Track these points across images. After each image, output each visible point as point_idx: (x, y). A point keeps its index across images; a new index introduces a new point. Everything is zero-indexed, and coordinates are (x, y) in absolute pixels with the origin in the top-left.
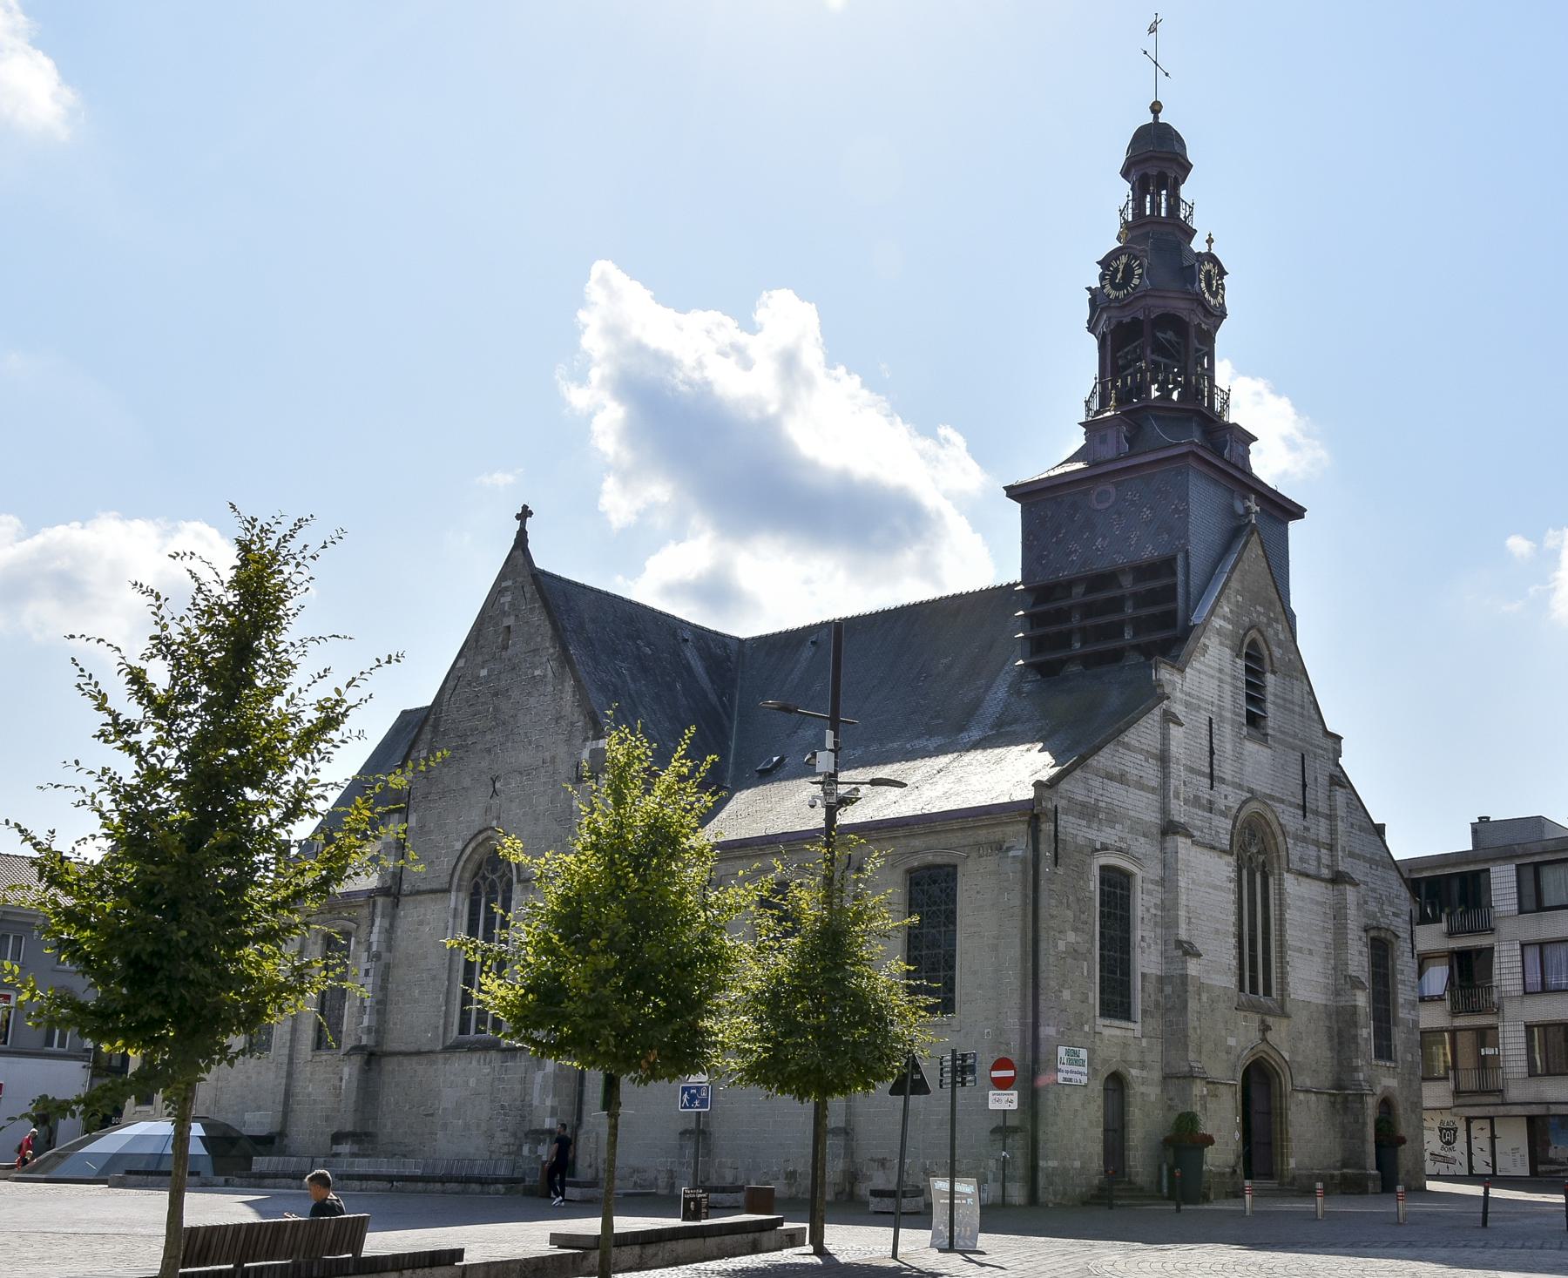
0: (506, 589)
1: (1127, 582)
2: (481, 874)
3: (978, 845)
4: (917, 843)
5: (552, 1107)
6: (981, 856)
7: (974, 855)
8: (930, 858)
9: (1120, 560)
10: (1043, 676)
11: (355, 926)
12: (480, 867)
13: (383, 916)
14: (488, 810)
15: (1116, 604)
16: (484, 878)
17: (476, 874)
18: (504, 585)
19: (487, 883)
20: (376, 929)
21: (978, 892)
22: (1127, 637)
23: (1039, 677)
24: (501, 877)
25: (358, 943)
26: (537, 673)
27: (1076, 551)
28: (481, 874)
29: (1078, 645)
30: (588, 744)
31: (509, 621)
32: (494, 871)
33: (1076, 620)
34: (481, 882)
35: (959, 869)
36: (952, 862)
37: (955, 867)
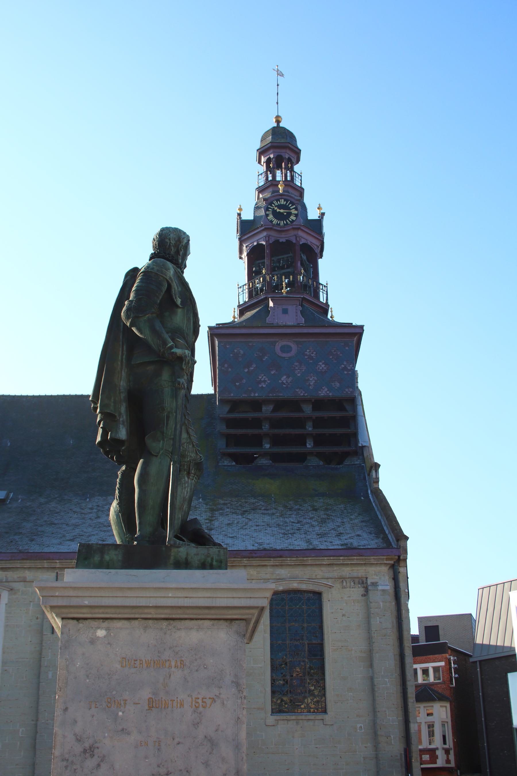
1: (308, 409)
3: (342, 579)
4: (283, 572)
6: (344, 587)
7: (338, 585)
8: (295, 585)
9: (301, 393)
10: (237, 463)
21: (343, 615)
22: (308, 446)
23: (234, 463)
27: (265, 381)
29: (267, 446)
33: (266, 428)
35: (325, 597)
36: (316, 589)
37: (318, 595)
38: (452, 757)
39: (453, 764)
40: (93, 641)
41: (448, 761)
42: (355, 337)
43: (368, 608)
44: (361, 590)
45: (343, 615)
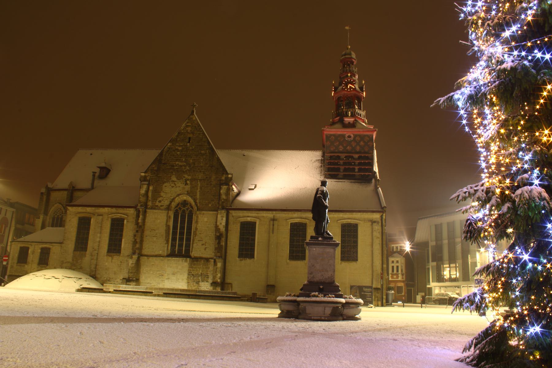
0: (189, 126)
2: (179, 207)
5: (220, 277)
6: (365, 222)
8: (349, 221)
11: (126, 216)
12: (178, 205)
13: (143, 215)
14: (183, 188)
15: (360, 164)
16: (180, 209)
17: (176, 207)
18: (188, 124)
19: (182, 210)
20: (140, 219)
21: (364, 231)
24: (187, 209)
25: (128, 222)
26: (202, 152)
27: (341, 148)
28: (179, 207)
30: (224, 175)
31: (191, 136)
32: (184, 207)
34: (179, 209)
38: (404, 277)
39: (404, 279)
40: (313, 250)
41: (403, 278)
42: (374, 132)
43: (372, 229)
44: (370, 223)
45: (364, 231)
